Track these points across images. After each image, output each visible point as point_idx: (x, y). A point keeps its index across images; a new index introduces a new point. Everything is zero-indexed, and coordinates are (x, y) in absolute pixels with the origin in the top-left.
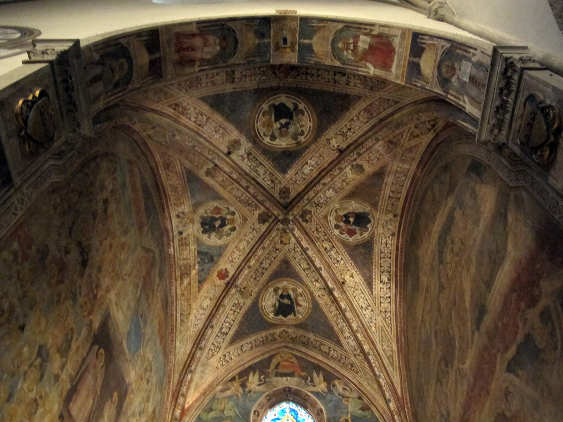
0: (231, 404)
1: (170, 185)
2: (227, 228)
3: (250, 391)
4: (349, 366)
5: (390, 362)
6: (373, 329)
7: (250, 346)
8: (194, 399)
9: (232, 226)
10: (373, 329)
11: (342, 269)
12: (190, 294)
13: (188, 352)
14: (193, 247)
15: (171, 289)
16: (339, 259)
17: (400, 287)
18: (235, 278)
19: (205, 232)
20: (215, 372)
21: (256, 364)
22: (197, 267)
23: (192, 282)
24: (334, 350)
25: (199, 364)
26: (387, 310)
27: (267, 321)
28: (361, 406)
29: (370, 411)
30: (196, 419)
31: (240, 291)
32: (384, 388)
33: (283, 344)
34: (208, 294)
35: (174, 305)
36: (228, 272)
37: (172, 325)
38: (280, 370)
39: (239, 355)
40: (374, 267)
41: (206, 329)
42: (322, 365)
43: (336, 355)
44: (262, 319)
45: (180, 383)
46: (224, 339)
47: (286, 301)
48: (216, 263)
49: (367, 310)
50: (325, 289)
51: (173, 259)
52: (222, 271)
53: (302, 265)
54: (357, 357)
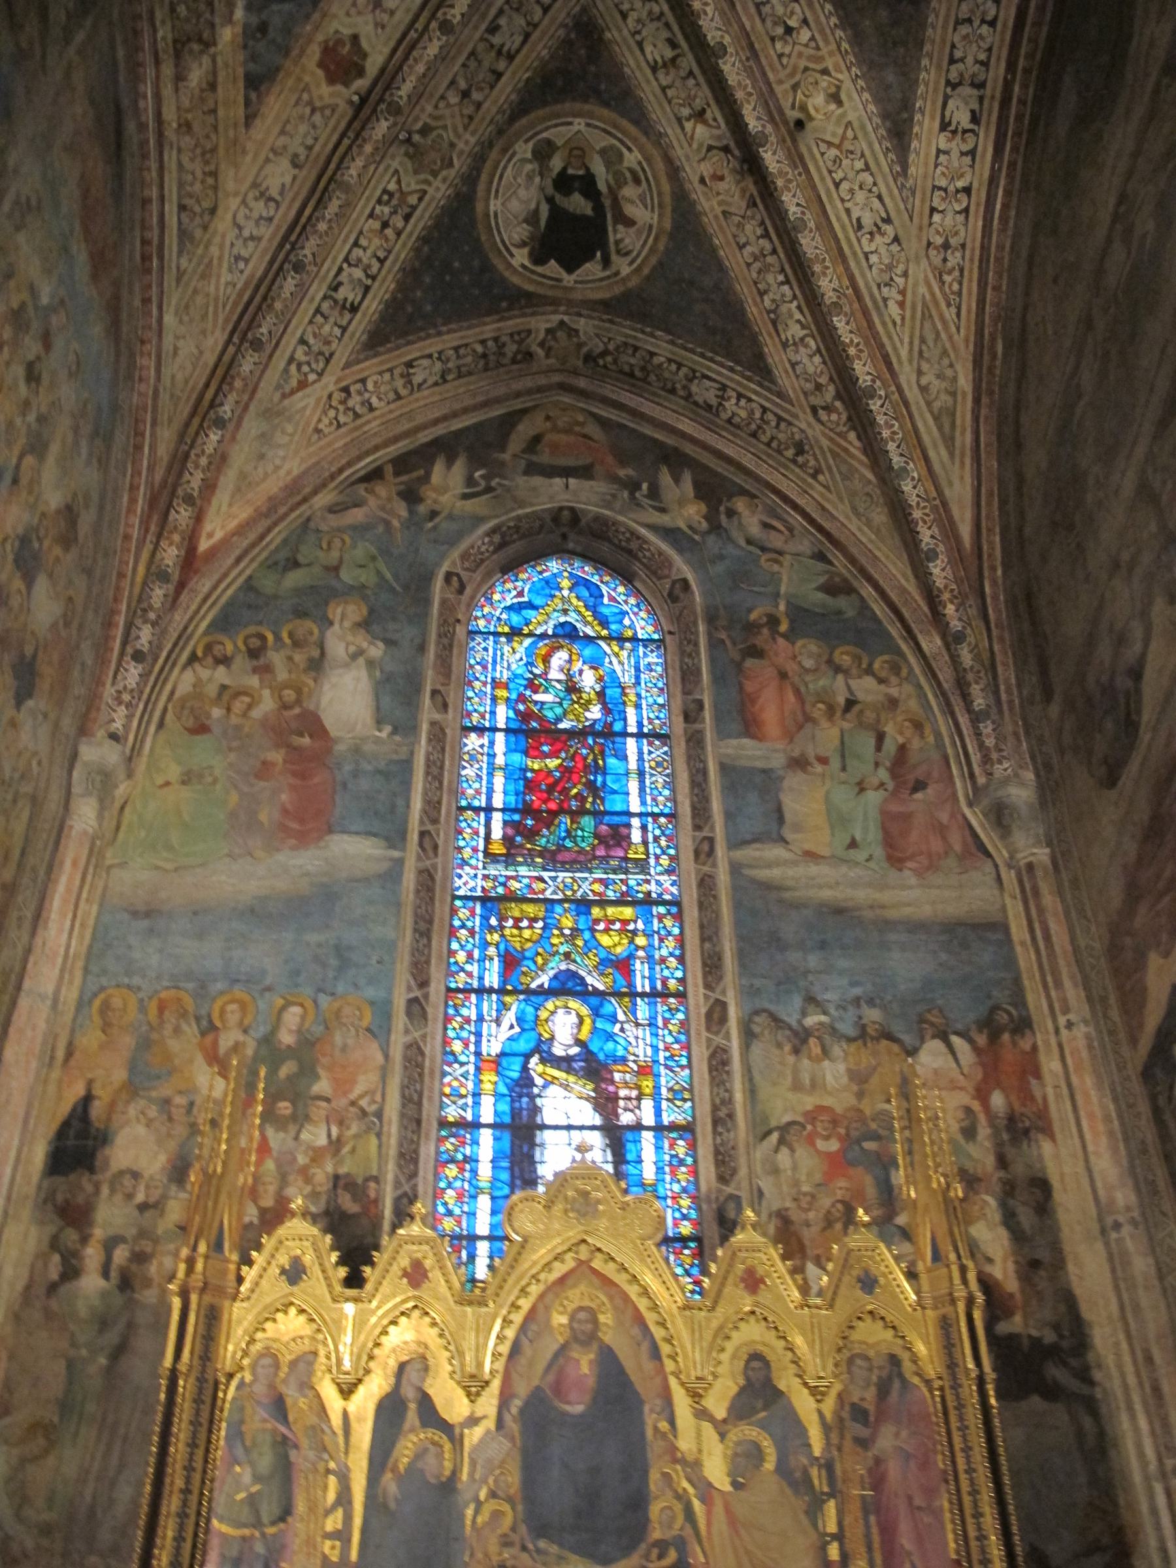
0: (361, 551)
3: (434, 514)
4: (790, 453)
5: (940, 428)
6: (894, 310)
7: (438, 366)
8: (232, 524)
10: (894, 310)
11: (803, 63)
13: (210, 359)
15: (137, 96)
16: (792, 23)
17: (1015, 149)
18: (389, 77)
20: (309, 444)
21: (458, 434)
22: (239, 14)
23: (220, 79)
24: (740, 396)
25: (252, 408)
26: (953, 241)
27: (503, 280)
28: (822, 580)
29: (854, 596)
30: (240, 589)
31: (408, 141)
32: (917, 514)
33: (556, 378)
34: (282, 141)
37: (145, 242)
38: (544, 457)
39: (399, 397)
40: (925, 62)
41: (277, 274)
42: (689, 449)
43: (743, 414)
44: (487, 267)
45: (180, 461)
46: (344, 329)
47: (578, 204)
49: (878, 237)
50: (726, 149)
52: (340, 42)
53: (648, 49)
54: (823, 415)
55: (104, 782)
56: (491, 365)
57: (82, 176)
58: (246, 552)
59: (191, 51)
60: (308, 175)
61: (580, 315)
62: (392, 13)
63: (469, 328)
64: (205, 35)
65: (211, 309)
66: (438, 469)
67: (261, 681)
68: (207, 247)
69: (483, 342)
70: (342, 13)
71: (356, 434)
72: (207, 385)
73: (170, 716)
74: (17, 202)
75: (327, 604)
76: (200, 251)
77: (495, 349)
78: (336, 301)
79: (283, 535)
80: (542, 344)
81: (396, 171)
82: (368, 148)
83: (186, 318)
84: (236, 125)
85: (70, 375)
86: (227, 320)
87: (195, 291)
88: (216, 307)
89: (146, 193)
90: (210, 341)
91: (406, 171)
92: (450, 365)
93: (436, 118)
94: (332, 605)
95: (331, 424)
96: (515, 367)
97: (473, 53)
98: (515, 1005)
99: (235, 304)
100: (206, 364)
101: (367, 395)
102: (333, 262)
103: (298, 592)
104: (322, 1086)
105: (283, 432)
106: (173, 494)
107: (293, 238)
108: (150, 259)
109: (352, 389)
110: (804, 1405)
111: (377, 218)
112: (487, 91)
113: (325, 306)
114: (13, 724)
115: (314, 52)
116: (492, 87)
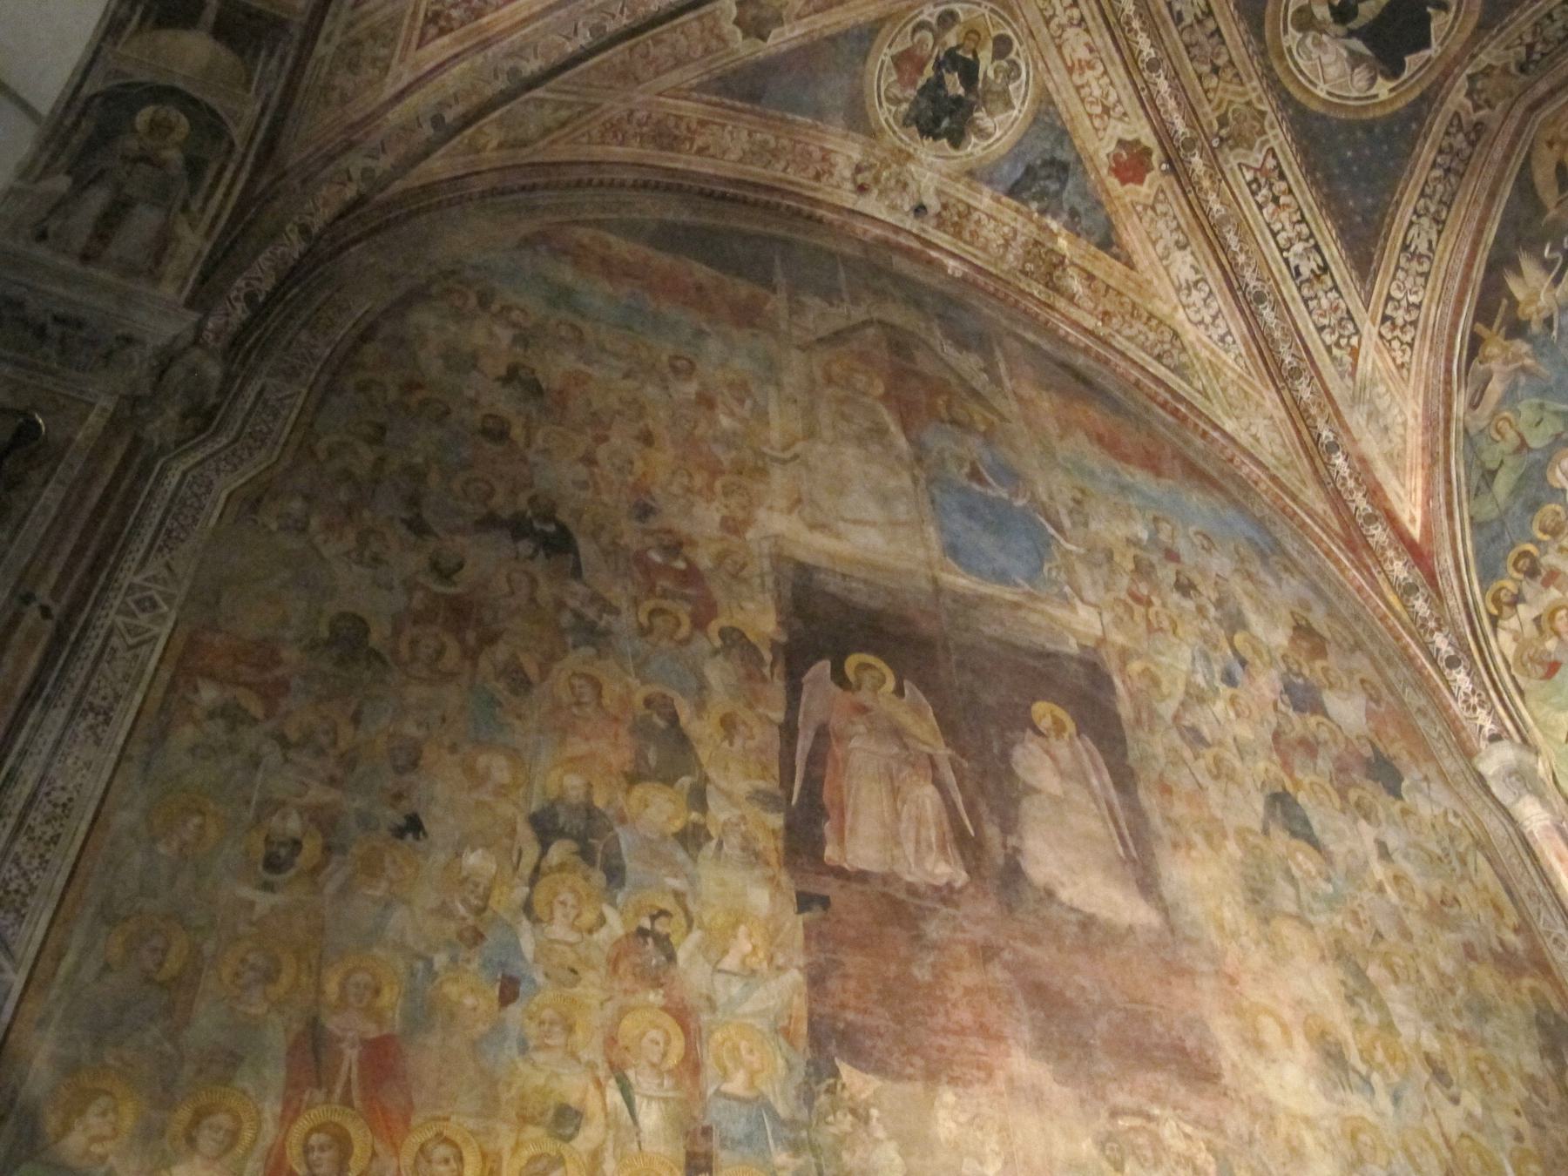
0: (1527, 412)
1: (740, 161)
2: (987, 65)
3: (1548, 322)
7: (1425, 221)
9: (990, 44)
12: (1119, 294)
14: (985, 200)
15: (1063, 341)
18: (1164, 133)
19: (957, 139)
20: (1406, 381)
22: (1054, 225)
23: (1089, 268)
27: (1396, 113)
30: (1473, 535)
31: (1222, 140)
33: (1518, 111)
34: (1160, 247)
35: (1115, 359)
36: (1137, 142)
39: (1426, 275)
44: (1368, 127)
45: (1337, 500)
46: (1335, 288)
48: (1079, 160)
51: (981, 279)
52: (1116, 157)
55: (1522, 778)
56: (1461, 169)
57: (1087, 434)
58: (1449, 504)
59: (1059, 278)
60: (1198, 241)
61: (1474, 56)
62: (1119, 101)
63: (1412, 173)
64: (1055, 260)
65: (1246, 387)
66: (1514, 285)
67: (1558, 588)
68: (1198, 358)
69: (1434, 165)
70: (1097, 144)
71: (1429, 332)
72: (1298, 432)
73: (1521, 680)
74: (1070, 512)
75: (1545, 479)
76: (1198, 366)
77: (1448, 158)
78: (1308, 280)
79: (1461, 463)
80: (1477, 108)
81: (1240, 165)
82: (1206, 183)
83: (1237, 412)
84: (1127, 277)
85: (1208, 551)
86: (1262, 379)
87: (1224, 390)
88: (1246, 381)
89: (1132, 379)
90: (1268, 404)
91: (1245, 156)
92: (1432, 209)
93: (1219, 105)
94: (1549, 475)
95: (1404, 351)
96: (1478, 147)
97: (1187, 47)
99: (1255, 365)
100: (1282, 421)
101: (1404, 303)
102: (1276, 261)
103: (1515, 492)
105: (1379, 396)
106: (1358, 528)
107: (1236, 285)
108: (1177, 410)
109: (1389, 312)
111: (1266, 202)
112: (1224, 50)
113: (1305, 292)
114: (1405, 812)
115: (1113, 182)
116: (1223, 43)
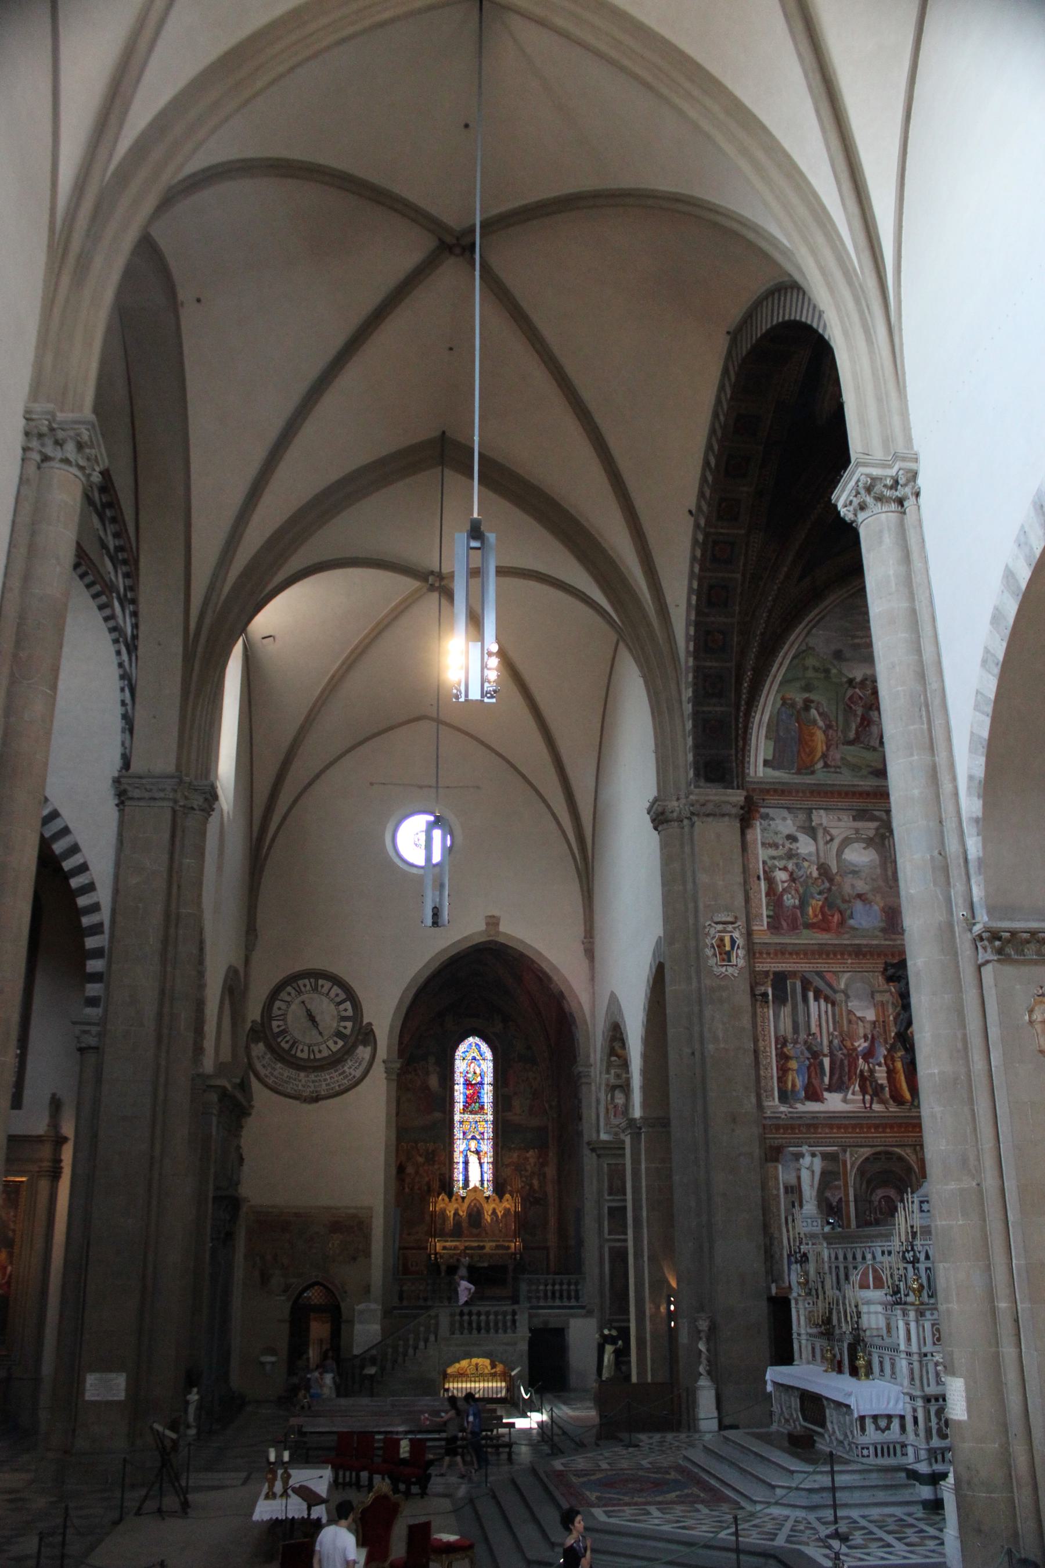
98: (465, 1141)
104: (436, 1159)
110: (500, 1215)
